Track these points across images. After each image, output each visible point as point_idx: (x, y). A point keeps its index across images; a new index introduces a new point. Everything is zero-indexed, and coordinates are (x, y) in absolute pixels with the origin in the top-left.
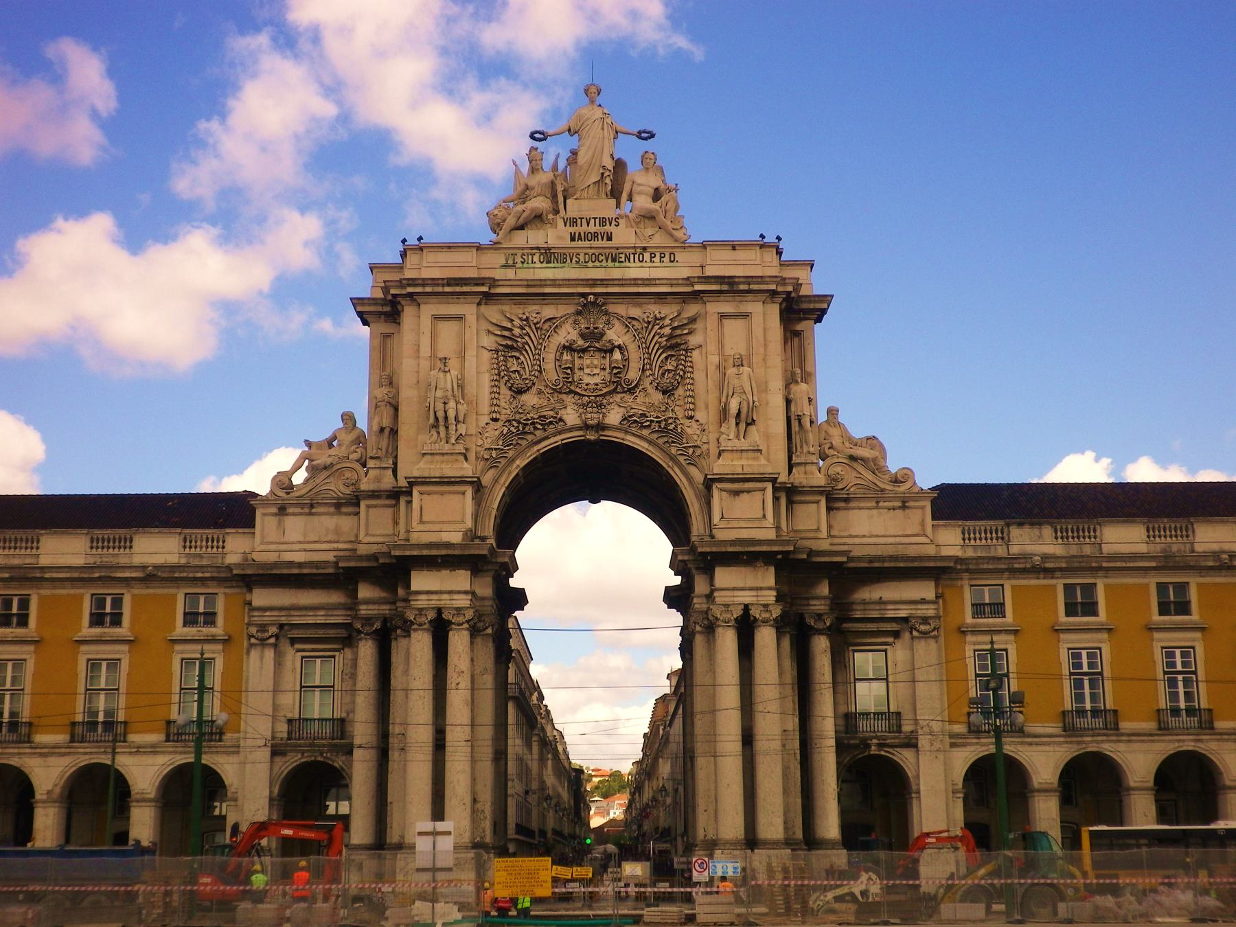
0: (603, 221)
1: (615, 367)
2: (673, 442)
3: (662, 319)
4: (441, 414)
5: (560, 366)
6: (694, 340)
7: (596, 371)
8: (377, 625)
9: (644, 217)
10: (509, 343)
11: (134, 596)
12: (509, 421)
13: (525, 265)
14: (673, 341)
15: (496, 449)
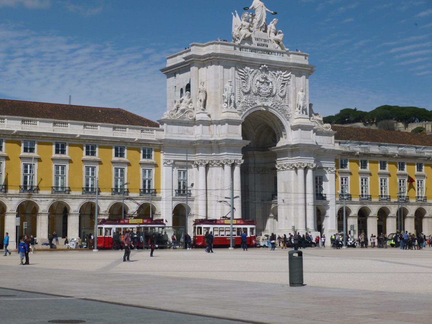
0: (265, 41)
1: (270, 89)
2: (283, 113)
3: (281, 74)
4: (229, 99)
5: (256, 86)
6: (289, 83)
7: (266, 89)
8: (207, 163)
9: (275, 40)
10: (244, 77)
11: (127, 147)
12: (243, 102)
13: (245, 52)
14: (284, 82)
15: (240, 111)
